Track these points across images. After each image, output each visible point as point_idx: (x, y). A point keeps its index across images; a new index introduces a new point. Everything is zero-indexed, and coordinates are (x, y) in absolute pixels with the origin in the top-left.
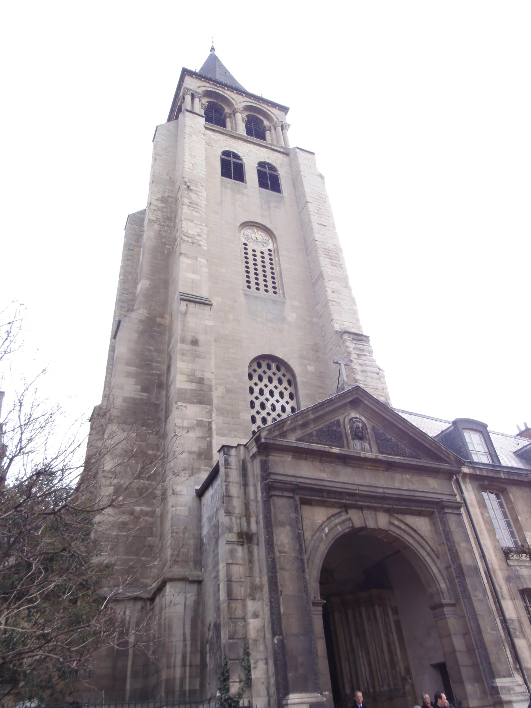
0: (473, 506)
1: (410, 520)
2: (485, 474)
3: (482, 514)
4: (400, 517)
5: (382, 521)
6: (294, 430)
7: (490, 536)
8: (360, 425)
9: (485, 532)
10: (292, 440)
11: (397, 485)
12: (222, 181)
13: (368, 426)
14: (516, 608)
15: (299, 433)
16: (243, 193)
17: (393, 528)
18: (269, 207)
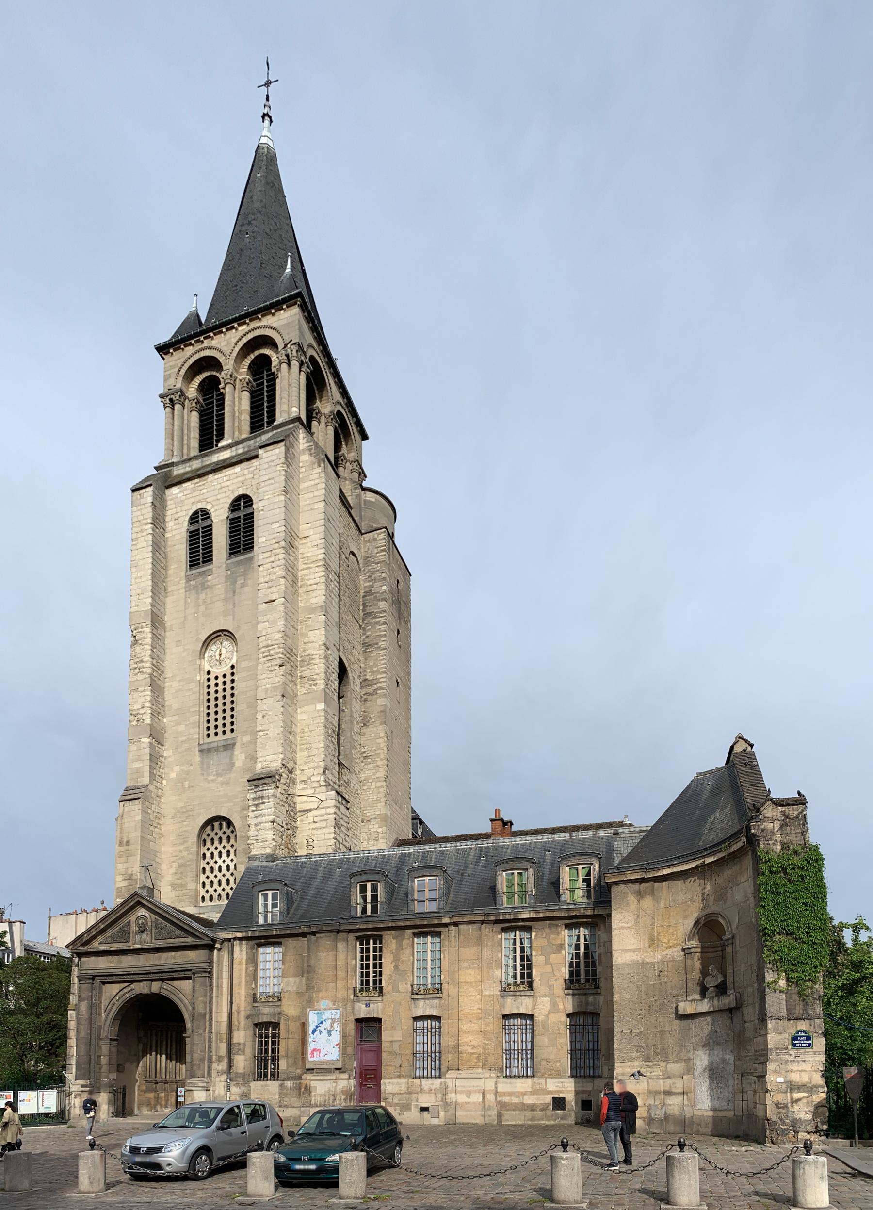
0: (240, 963)
1: (176, 983)
2: (257, 934)
3: (247, 969)
4: (169, 982)
5: (155, 987)
6: (94, 937)
7: (246, 985)
8: (140, 922)
9: (243, 983)
10: (95, 946)
11: (162, 962)
12: (188, 579)
13: (149, 920)
14: (246, 1036)
15: (100, 939)
16: (208, 587)
17: (162, 990)
18: (234, 592)
